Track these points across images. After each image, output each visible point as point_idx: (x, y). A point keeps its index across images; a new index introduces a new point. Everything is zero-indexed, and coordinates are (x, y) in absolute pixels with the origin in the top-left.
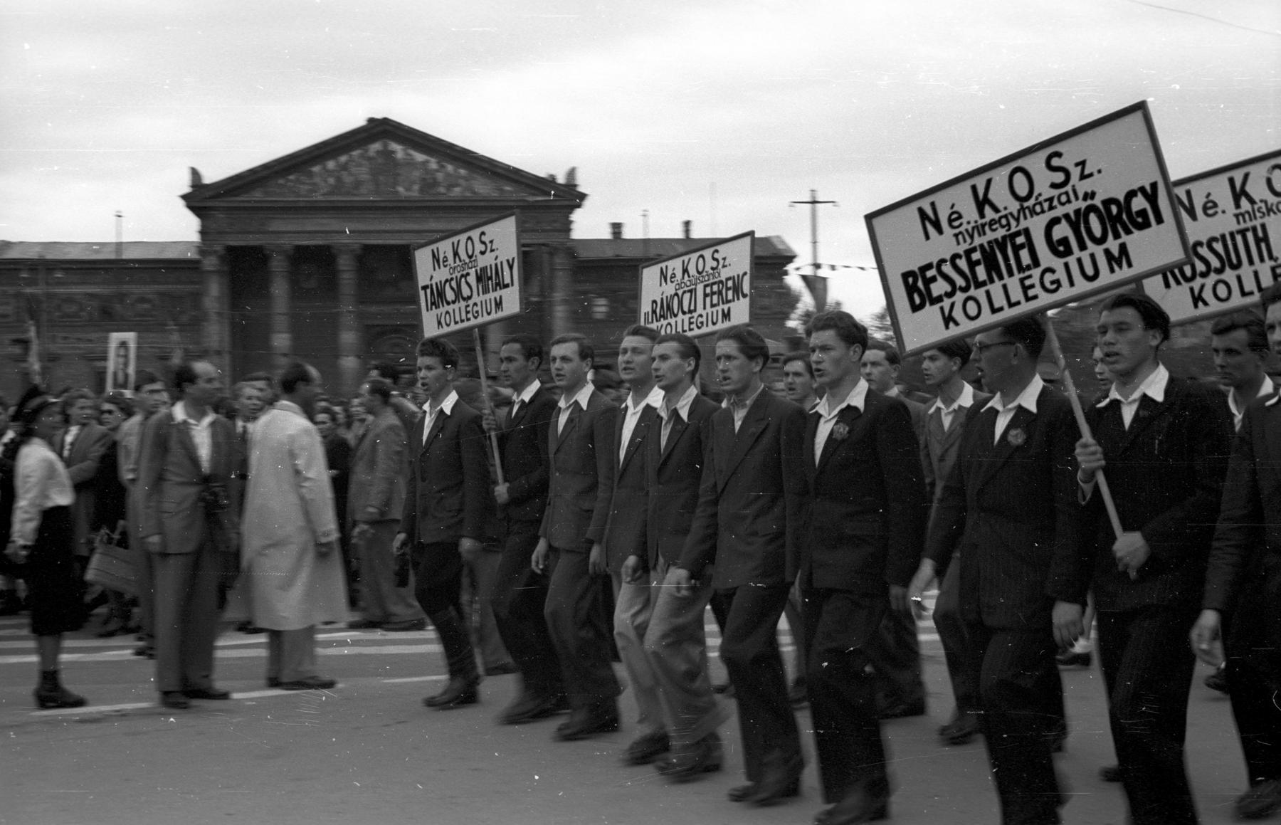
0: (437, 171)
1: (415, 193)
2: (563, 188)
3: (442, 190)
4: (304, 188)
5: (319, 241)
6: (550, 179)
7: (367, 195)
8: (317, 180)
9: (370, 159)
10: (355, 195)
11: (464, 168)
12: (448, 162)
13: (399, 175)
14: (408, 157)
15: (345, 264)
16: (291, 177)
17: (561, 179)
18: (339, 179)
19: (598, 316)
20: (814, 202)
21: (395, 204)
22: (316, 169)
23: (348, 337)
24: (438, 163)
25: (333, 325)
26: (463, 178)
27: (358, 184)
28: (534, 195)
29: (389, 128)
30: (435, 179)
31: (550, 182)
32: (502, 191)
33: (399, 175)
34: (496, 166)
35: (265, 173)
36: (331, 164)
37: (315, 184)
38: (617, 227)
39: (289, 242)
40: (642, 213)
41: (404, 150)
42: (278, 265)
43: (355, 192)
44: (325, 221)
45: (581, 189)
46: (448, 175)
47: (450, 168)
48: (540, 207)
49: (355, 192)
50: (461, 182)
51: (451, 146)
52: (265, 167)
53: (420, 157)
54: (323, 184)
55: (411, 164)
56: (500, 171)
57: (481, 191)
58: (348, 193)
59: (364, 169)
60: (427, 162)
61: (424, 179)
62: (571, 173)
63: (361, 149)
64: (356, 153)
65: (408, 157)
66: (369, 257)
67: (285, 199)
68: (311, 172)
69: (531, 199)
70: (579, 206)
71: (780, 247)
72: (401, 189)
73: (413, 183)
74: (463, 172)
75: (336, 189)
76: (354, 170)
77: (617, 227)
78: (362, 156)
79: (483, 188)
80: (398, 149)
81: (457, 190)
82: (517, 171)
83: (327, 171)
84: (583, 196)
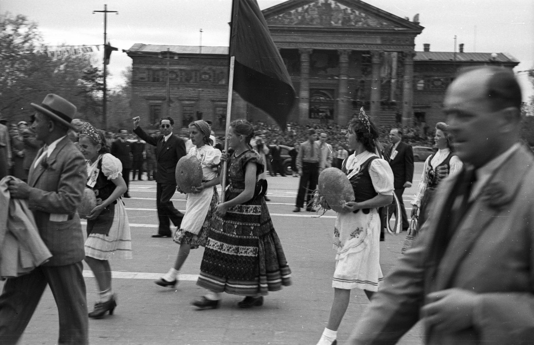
0: (351, 14)
1: (339, 24)
2: (413, 24)
3: (353, 23)
4: (287, 21)
5: (292, 47)
6: (406, 19)
7: (316, 24)
8: (293, 17)
9: (318, 7)
11: (364, 13)
12: (357, 10)
13: (332, 15)
14: (337, 7)
15: (304, 58)
16: (281, 15)
17: (411, 20)
18: (303, 17)
19: (419, 89)
21: (329, 30)
22: (293, 11)
24: (351, 10)
27: (312, 20)
28: (397, 27)
30: (349, 18)
31: (406, 21)
32: (382, 24)
33: (332, 15)
34: (380, 12)
35: (268, 13)
36: (300, 9)
37: (292, 19)
40: (454, 37)
41: (335, 3)
43: (311, 23)
45: (421, 25)
46: (356, 16)
47: (357, 13)
49: (311, 23)
54: (295, 19)
55: (338, 10)
56: (381, 14)
57: (372, 25)
58: (308, 24)
59: (316, 12)
60: (346, 9)
61: (344, 18)
62: (417, 17)
64: (312, 4)
65: (337, 7)
66: (316, 54)
67: (277, 26)
68: (291, 13)
69: (396, 29)
70: (419, 33)
71: (510, 58)
72: (333, 22)
73: (339, 20)
74: (363, 15)
75: (302, 22)
76: (310, 12)
78: (314, 6)
79: (373, 22)
81: (360, 23)
82: (390, 15)
83: (298, 13)
84: (422, 28)
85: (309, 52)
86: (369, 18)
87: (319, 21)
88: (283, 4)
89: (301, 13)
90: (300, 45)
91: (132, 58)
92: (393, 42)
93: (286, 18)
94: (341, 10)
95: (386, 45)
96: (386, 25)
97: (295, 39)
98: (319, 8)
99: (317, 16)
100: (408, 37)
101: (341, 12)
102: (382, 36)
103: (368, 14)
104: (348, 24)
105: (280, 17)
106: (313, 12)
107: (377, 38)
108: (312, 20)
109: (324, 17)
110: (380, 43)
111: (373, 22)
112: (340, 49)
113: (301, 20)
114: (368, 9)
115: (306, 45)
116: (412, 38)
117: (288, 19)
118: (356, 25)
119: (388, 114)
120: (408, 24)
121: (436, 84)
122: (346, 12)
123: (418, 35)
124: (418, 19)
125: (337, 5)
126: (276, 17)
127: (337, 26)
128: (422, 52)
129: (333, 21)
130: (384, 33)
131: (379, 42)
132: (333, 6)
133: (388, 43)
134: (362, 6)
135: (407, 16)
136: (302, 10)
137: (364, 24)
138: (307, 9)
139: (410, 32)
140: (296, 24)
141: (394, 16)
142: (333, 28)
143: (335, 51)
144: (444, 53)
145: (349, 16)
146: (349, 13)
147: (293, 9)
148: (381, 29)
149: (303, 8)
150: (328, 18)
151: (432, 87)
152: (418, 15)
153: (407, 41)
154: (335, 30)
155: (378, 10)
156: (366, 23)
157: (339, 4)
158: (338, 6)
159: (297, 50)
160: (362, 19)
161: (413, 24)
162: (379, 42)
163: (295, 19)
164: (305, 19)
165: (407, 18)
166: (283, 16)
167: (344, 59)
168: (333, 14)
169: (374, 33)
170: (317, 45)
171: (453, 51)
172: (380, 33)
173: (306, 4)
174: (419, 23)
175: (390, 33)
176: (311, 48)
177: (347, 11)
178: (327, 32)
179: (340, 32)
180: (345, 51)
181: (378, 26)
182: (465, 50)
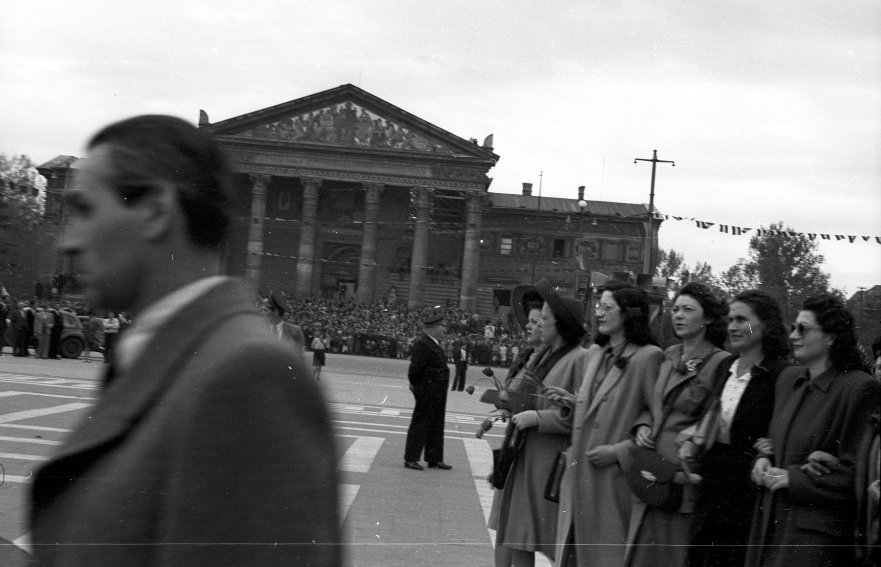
1: (368, 143)
2: (482, 150)
3: (389, 143)
5: (290, 174)
6: (472, 142)
7: (330, 141)
10: (323, 142)
11: (407, 128)
13: (357, 129)
14: (364, 116)
15: (309, 193)
16: (276, 124)
17: (481, 143)
18: (311, 129)
19: (503, 252)
20: (655, 161)
22: (294, 119)
23: (305, 249)
25: (296, 239)
26: (405, 135)
28: (460, 153)
29: (352, 92)
30: (384, 135)
33: (357, 129)
36: (306, 117)
37: (292, 130)
38: (527, 187)
39: (267, 173)
41: (362, 110)
42: (258, 189)
43: (322, 139)
44: (297, 159)
45: (494, 152)
46: (394, 131)
47: (396, 127)
48: (463, 163)
50: (404, 138)
51: (399, 110)
52: (255, 114)
53: (374, 117)
54: (298, 131)
55: (366, 120)
57: (418, 147)
58: (318, 140)
62: (489, 139)
63: (330, 107)
64: (325, 110)
68: (292, 121)
69: (455, 156)
70: (494, 165)
72: (357, 140)
73: (367, 136)
74: (405, 131)
75: (307, 136)
76: (322, 122)
77: (527, 187)
78: (328, 111)
79: (420, 144)
80: (359, 110)
81: (401, 144)
83: (303, 122)
84: (497, 158)
85: (317, 183)
86: (414, 137)
87: (335, 136)
88: (278, 107)
89: (308, 122)
90: (302, 172)
91: (46, 178)
92: (452, 176)
93: (283, 129)
94: (371, 122)
95: (438, 180)
96: (440, 149)
97: (294, 162)
98: (336, 117)
99: (332, 128)
100: (476, 170)
101: (372, 125)
102: (433, 166)
103: (414, 131)
104: (381, 144)
105: (274, 126)
106: (328, 122)
107: (425, 168)
108: (324, 133)
109: (344, 131)
110: (430, 176)
111: (420, 144)
112: (367, 182)
113: (306, 133)
114: (413, 122)
115: (312, 172)
116: (480, 172)
117: (286, 130)
118: (393, 146)
119: (445, 290)
120: (473, 148)
121: (529, 247)
122: (379, 125)
123: (492, 168)
124: (491, 143)
125: (364, 113)
126: (267, 127)
127: (362, 146)
128: (519, 196)
129: (358, 138)
130: (437, 161)
131: (428, 174)
132: (359, 114)
133: (443, 177)
134: (403, 118)
135: (474, 138)
136: (310, 118)
137: (407, 144)
138: (318, 117)
139: (478, 161)
140: (298, 139)
141: (452, 136)
142: (356, 149)
143: (359, 185)
144: (552, 199)
145: (385, 131)
146: (384, 128)
147: (295, 115)
148: (432, 155)
149: (311, 115)
150: (350, 132)
151: (525, 251)
152: (492, 135)
153: (472, 175)
154: (359, 152)
155: (428, 124)
156: (409, 143)
157: (367, 112)
158: (367, 115)
159: (296, 180)
160: (404, 138)
161: (482, 150)
162: (428, 174)
163: (298, 131)
164: (313, 131)
165: (476, 139)
166: (279, 125)
167: (371, 198)
168: (358, 126)
169: (420, 159)
170: (330, 174)
171: (538, 195)
172: (431, 160)
173: (315, 109)
174: (492, 149)
175: (448, 162)
176: (319, 178)
177: (381, 124)
178: (347, 154)
179: (367, 155)
180: (373, 185)
181: (429, 150)
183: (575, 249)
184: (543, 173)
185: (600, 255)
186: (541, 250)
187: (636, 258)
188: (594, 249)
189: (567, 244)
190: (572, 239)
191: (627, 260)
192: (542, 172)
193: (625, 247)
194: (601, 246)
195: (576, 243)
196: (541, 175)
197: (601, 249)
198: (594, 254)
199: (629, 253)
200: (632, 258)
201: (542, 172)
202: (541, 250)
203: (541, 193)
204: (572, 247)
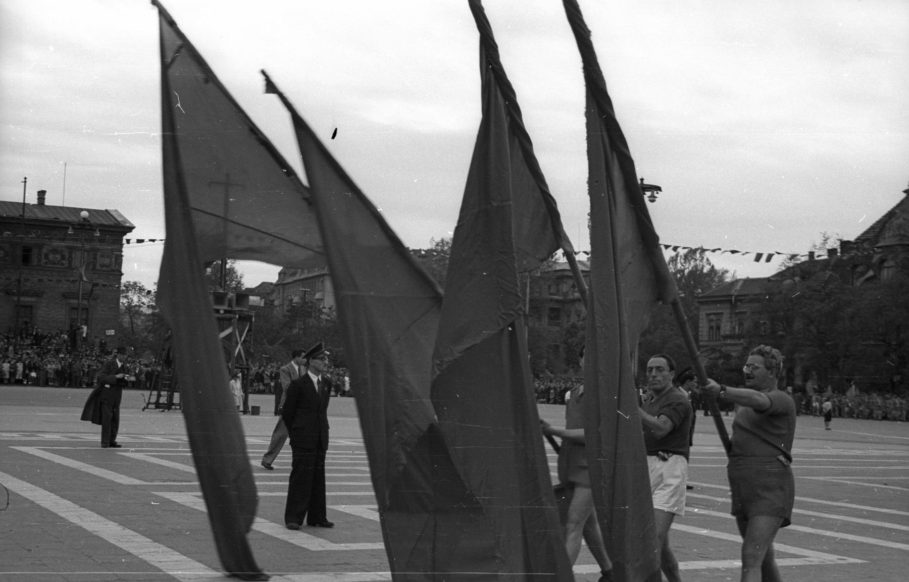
40: (24, 180)
71: (119, 219)
182: (47, 203)
183: (43, 256)
184: (27, 180)
185: (70, 263)
186: (7, 258)
187: (107, 267)
188: (63, 257)
189: (35, 251)
190: (40, 247)
191: (98, 267)
192: (25, 178)
193: (95, 255)
194: (70, 253)
195: (44, 251)
196: (25, 182)
197: (70, 257)
198: (64, 262)
199: (100, 261)
200: (102, 266)
201: (25, 178)
202: (7, 258)
203: (26, 200)
204: (40, 255)
